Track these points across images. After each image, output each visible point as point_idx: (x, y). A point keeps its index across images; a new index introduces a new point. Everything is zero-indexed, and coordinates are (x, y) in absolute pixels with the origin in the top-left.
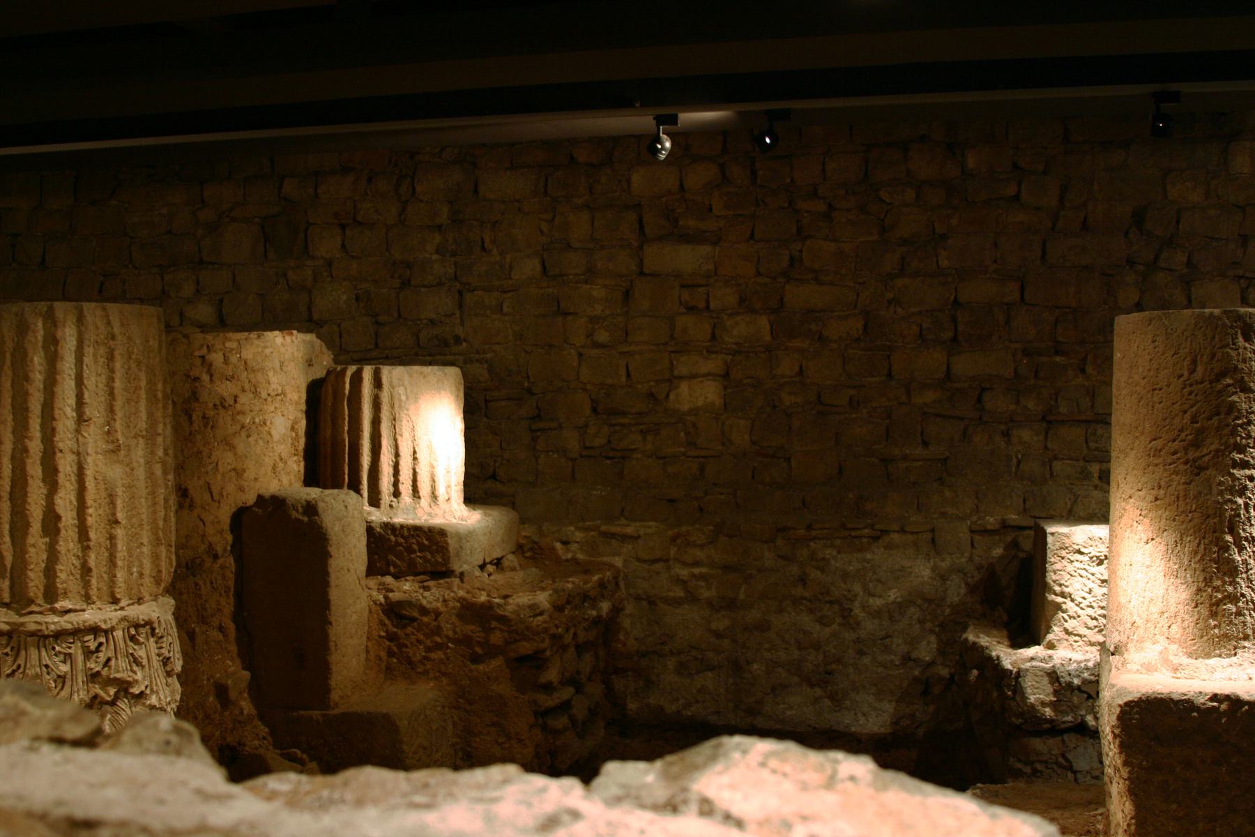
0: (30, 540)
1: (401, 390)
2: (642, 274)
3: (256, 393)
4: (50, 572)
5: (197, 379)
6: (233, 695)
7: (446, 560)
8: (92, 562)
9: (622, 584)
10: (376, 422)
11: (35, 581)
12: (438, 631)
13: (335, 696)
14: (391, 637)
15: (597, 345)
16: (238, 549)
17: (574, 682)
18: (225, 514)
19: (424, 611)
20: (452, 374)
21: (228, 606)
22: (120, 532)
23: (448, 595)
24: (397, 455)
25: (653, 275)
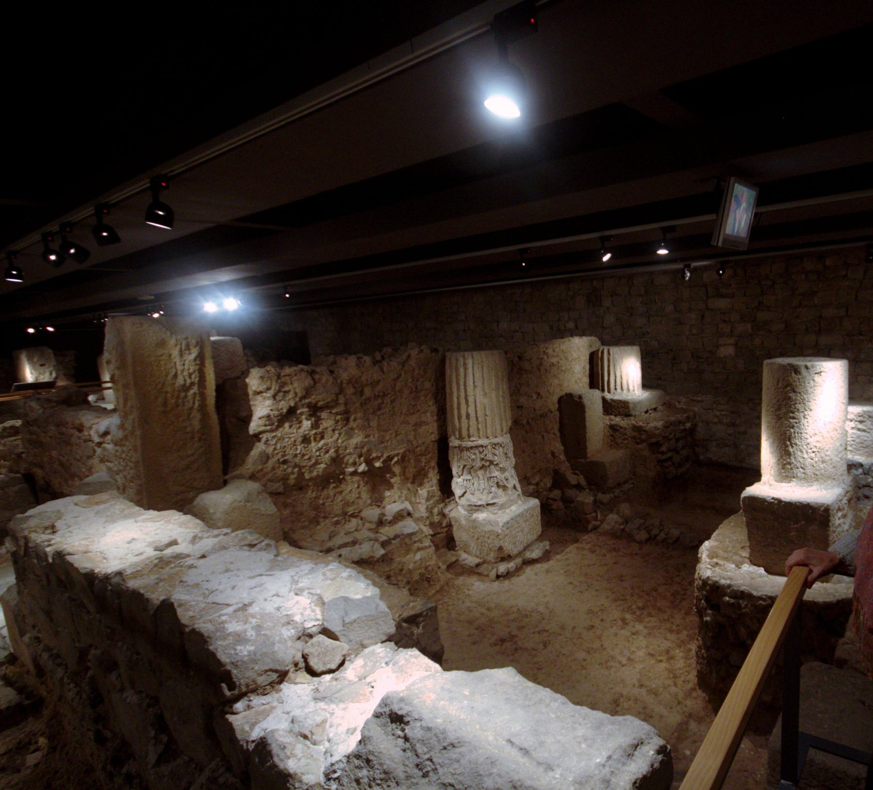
0: (462, 421)
1: (616, 356)
2: (707, 309)
3: (567, 359)
4: (468, 430)
5: (541, 359)
6: (556, 454)
7: (629, 412)
8: (480, 427)
9: (697, 417)
10: (609, 366)
11: (464, 433)
12: (625, 434)
13: (589, 455)
14: (612, 436)
15: (693, 334)
16: (560, 409)
17: (676, 451)
18: (555, 398)
19: (621, 428)
20: (636, 348)
21: (556, 427)
22: (487, 418)
23: (629, 422)
25: (712, 310)
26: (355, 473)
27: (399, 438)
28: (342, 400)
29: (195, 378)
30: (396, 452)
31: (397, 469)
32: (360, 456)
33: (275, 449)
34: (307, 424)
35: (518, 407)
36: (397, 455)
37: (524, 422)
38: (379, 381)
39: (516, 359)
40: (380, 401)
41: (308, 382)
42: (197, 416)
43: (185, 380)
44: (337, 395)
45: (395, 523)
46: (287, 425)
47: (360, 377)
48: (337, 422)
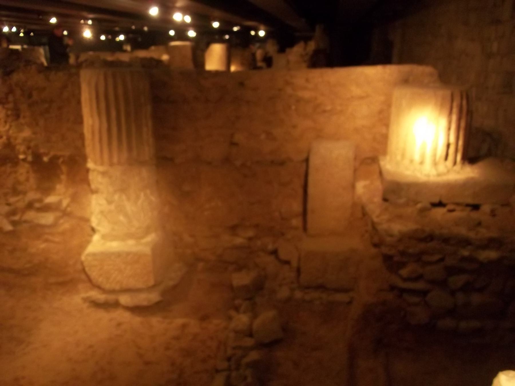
26: (24, 160)
28: (11, 98)
31: (64, 168)
32: (29, 148)
37: (238, 163)
40: (46, 106)
44: (7, 94)
48: (8, 116)
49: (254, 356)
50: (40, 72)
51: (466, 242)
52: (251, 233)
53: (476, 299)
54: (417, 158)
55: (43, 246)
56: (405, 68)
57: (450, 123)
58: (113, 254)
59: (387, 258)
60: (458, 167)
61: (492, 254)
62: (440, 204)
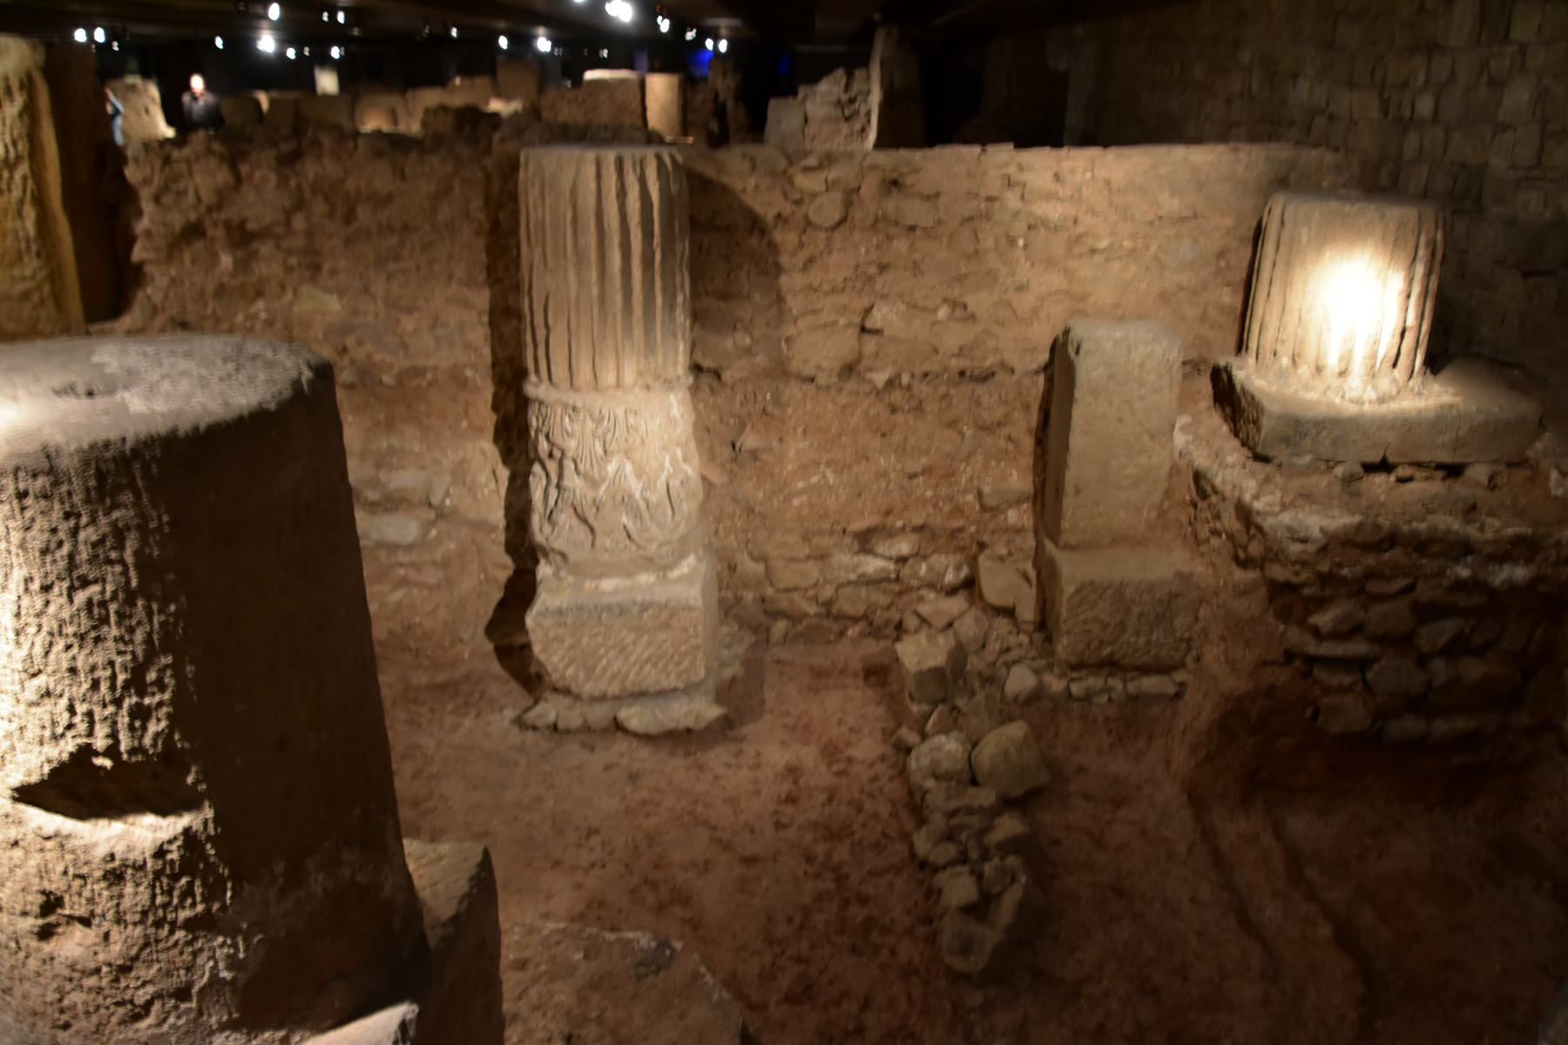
5: (990, 199)
24: (1284, 308)
27: (440, 332)
28: (299, 222)
29: (23, 147)
30: (431, 363)
33: (166, 297)
34: (226, 261)
35: (863, 329)
36: (435, 369)
37: (880, 378)
38: (389, 198)
39: (870, 186)
41: (223, 176)
42: (30, 213)
43: (7, 151)
44: (288, 214)
45: (387, 510)
46: (187, 257)
47: (342, 181)
48: (289, 270)
49: (1008, 826)
50: (379, 154)
51: (1463, 548)
52: (904, 547)
53: (1473, 670)
54: (1332, 362)
55: (396, 596)
56: (1281, 152)
57: (1410, 281)
58: (609, 608)
59: (1281, 593)
60: (1415, 382)
61: (1520, 573)
62: (1384, 466)
